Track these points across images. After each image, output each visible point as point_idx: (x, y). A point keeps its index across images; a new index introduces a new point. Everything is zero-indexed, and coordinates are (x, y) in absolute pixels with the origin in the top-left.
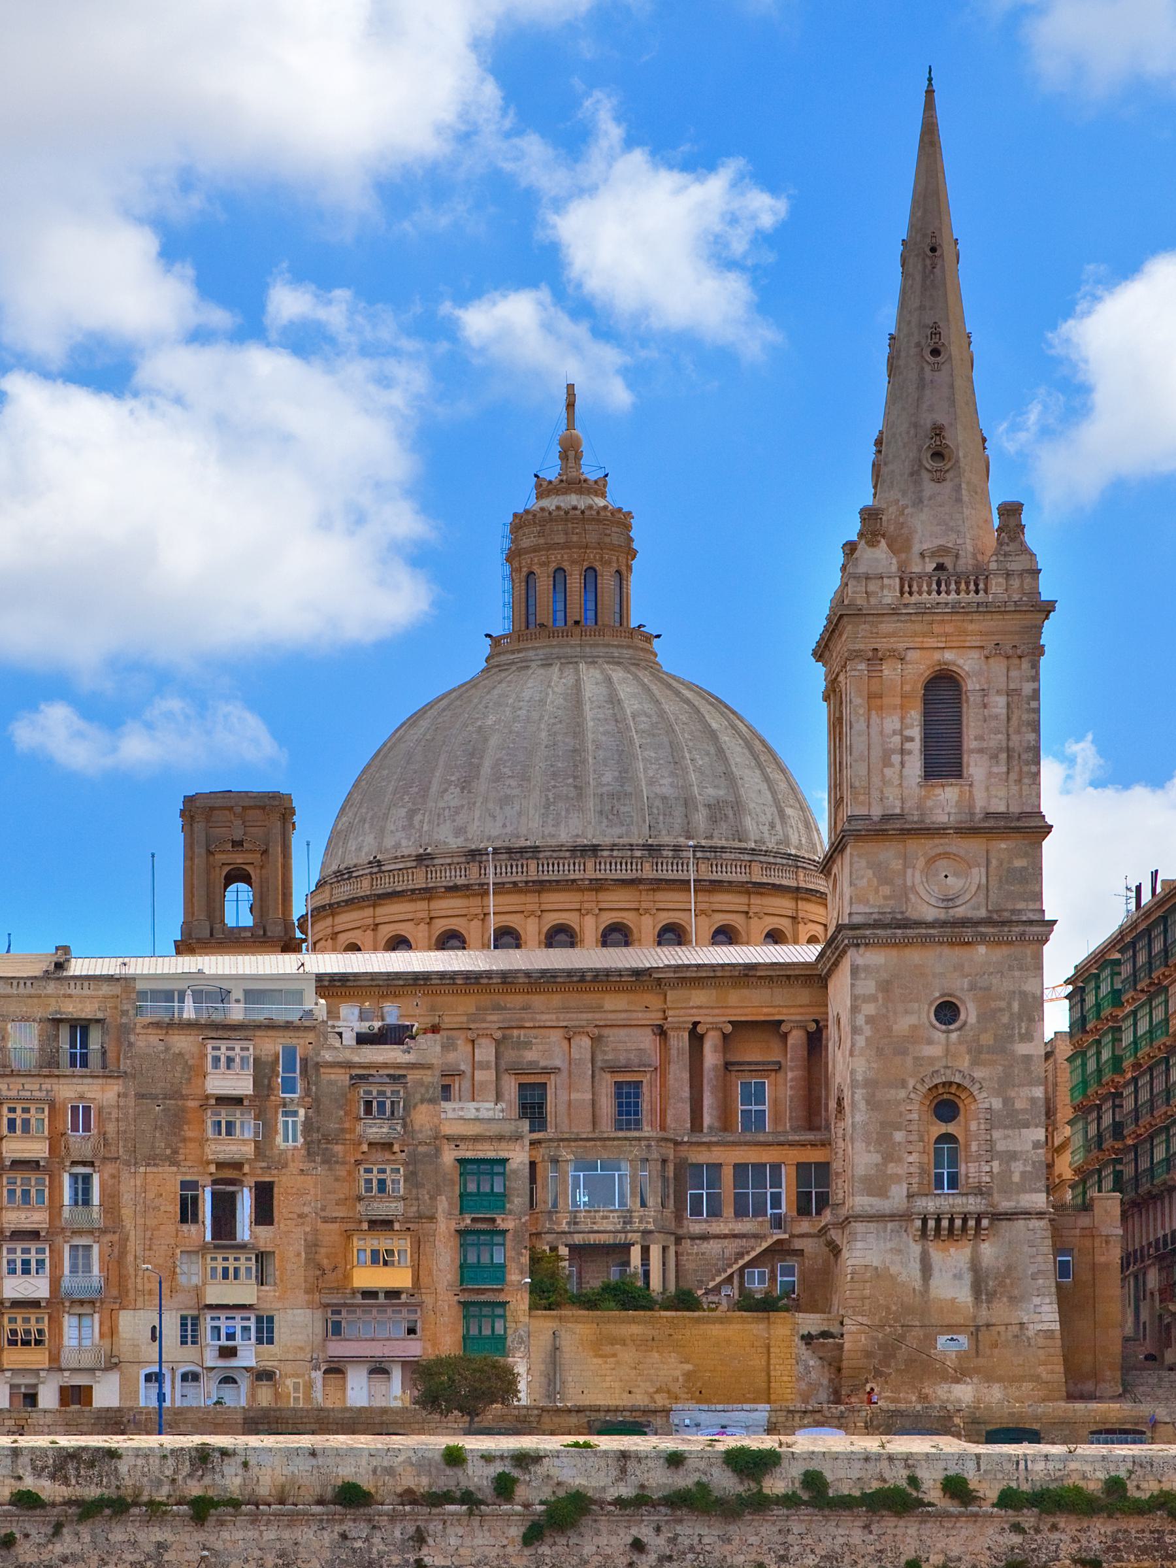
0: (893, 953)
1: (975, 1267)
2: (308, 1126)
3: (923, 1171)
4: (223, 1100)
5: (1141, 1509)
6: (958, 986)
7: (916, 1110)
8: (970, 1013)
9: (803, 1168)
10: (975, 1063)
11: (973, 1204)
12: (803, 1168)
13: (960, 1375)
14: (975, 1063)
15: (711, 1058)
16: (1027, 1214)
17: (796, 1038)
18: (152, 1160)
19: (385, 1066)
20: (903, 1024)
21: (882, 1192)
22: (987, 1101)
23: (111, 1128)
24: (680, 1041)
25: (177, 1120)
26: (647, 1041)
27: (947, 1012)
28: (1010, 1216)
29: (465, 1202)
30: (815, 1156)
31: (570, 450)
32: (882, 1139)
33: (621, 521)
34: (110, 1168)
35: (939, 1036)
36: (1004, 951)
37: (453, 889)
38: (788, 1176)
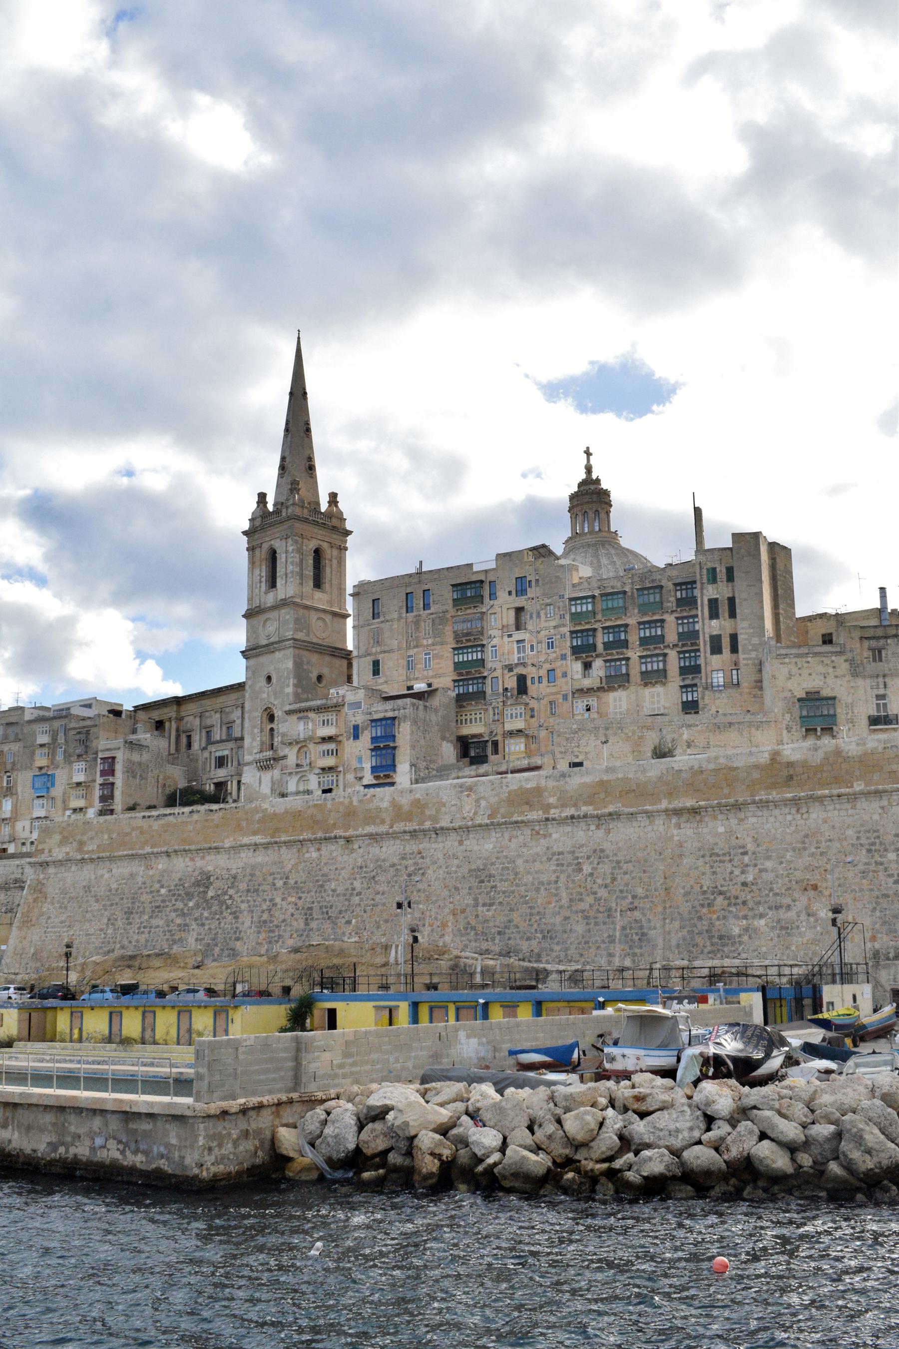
0: (255, 659)
1: (272, 777)
2: (65, 752)
3: (262, 744)
4: (42, 746)
8: (274, 680)
10: (275, 698)
14: (275, 698)
18: (26, 769)
19: (84, 727)
21: (250, 754)
23: (16, 759)
25: (33, 754)
27: (269, 679)
29: (103, 773)
31: (589, 469)
33: (606, 493)
34: (15, 773)
35: (266, 689)
36: (283, 652)
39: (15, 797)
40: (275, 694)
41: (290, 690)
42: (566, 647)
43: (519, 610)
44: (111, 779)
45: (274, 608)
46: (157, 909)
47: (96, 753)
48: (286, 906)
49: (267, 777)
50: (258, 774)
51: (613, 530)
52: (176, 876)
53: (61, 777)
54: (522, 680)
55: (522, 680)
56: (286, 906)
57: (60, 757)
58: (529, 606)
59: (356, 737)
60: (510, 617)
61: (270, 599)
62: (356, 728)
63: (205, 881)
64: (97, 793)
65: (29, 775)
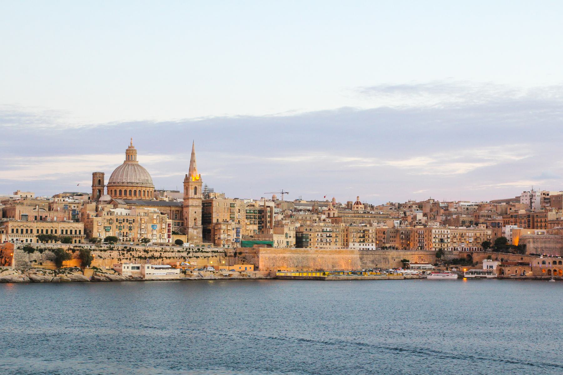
5: (219, 252)
6: (196, 211)
7: (193, 220)
8: (197, 213)
9: (182, 222)
11: (197, 227)
12: (182, 222)
13: (196, 240)
15: (174, 213)
16: (199, 228)
17: (180, 212)
20: (192, 213)
22: (198, 219)
24: (172, 212)
26: (169, 211)
27: (195, 212)
28: (199, 228)
30: (182, 221)
31: (131, 144)
32: (191, 223)
37: (126, 186)
38: (181, 223)
39: (187, 235)
40: (197, 215)
41: (201, 215)
42: (245, 217)
43: (239, 209)
44: (169, 228)
45: (197, 199)
46: (279, 261)
47: (166, 222)
48: (295, 261)
49: (195, 231)
50: (193, 230)
51: (137, 160)
52: (281, 257)
53: (159, 226)
54: (239, 221)
55: (239, 221)
56: (295, 261)
57: (158, 222)
58: (240, 209)
59: (233, 230)
60: (238, 210)
61: (196, 197)
62: (233, 228)
63: (284, 258)
64: (167, 231)
65: (151, 225)
